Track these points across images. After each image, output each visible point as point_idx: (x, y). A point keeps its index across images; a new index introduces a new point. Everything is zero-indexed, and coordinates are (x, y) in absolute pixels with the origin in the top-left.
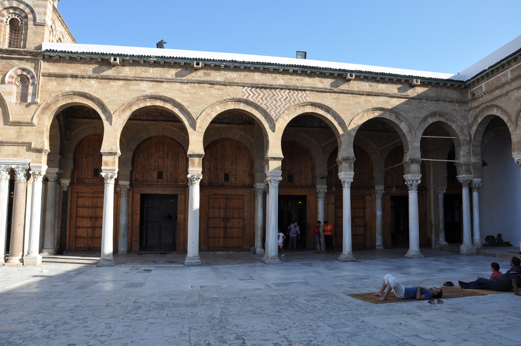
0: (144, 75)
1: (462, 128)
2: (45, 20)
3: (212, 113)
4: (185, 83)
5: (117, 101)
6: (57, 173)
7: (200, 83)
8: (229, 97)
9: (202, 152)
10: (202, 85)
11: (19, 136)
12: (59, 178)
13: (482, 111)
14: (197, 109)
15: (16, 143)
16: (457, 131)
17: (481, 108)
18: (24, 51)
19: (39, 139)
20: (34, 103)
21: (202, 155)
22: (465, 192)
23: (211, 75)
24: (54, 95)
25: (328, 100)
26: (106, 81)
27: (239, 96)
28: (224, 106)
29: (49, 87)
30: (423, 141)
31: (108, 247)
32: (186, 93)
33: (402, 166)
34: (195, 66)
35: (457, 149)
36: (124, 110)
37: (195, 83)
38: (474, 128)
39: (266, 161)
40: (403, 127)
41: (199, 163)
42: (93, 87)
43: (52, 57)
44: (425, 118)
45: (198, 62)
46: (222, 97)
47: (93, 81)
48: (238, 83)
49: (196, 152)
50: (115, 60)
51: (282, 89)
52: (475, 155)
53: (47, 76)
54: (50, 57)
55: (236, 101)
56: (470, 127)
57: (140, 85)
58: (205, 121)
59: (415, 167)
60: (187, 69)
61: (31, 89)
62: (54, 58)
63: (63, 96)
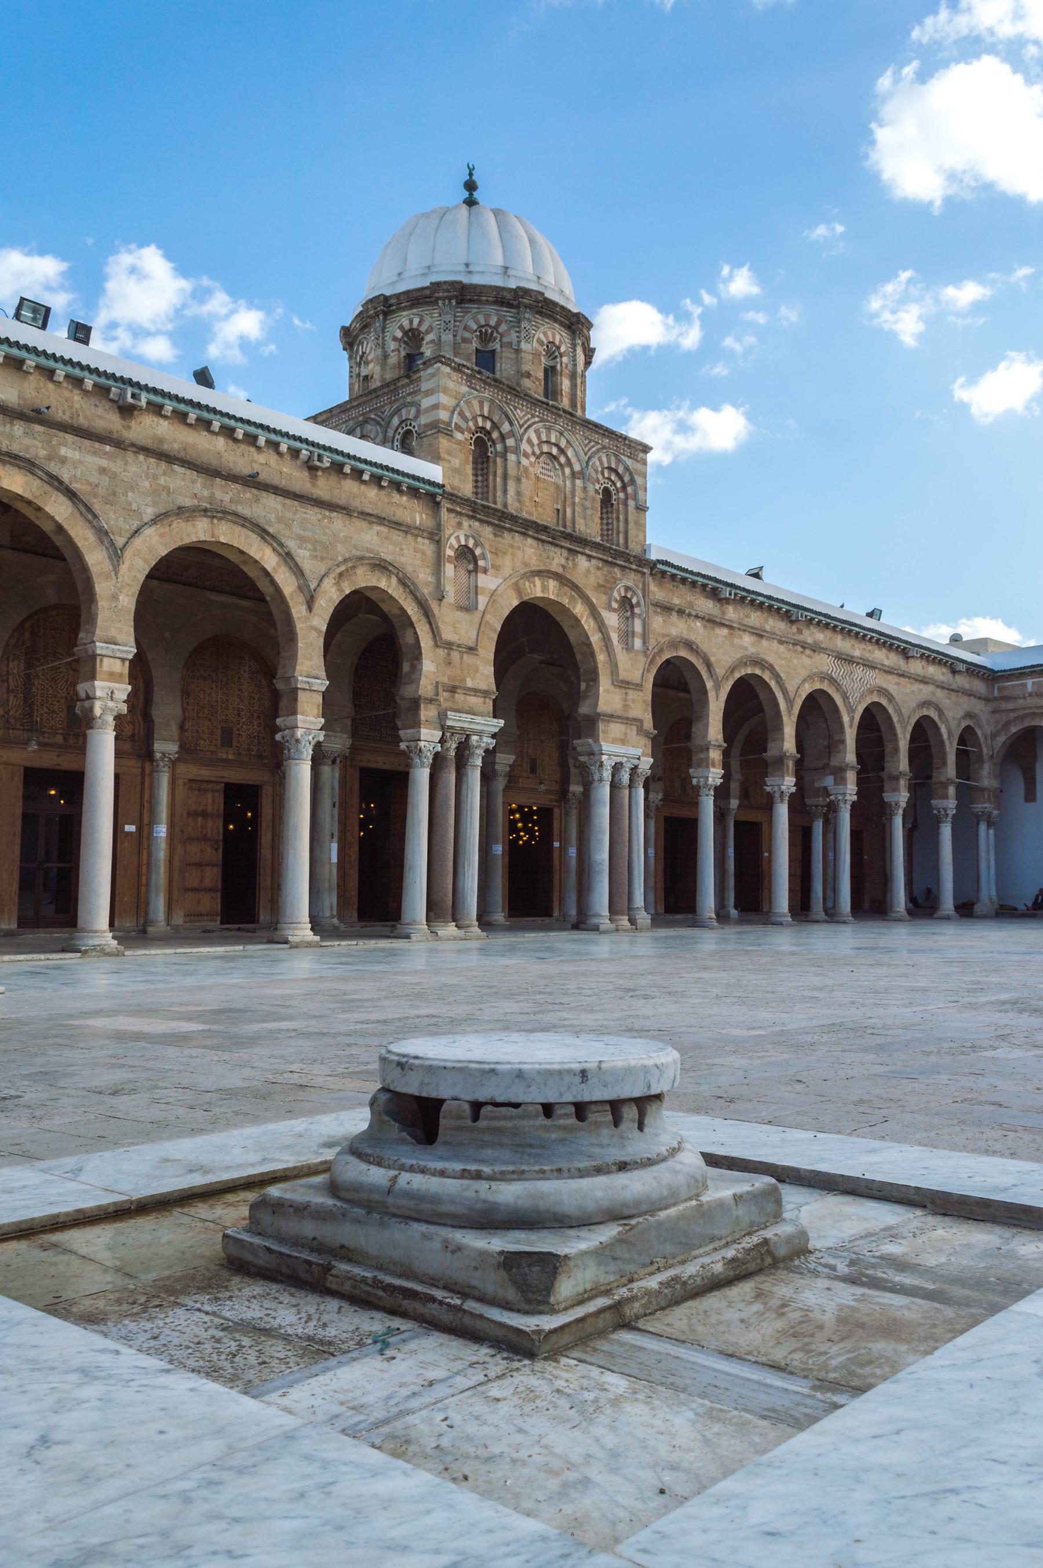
0: (747, 621)
1: (986, 738)
11: (626, 707)
16: (982, 740)
17: (1021, 713)
22: (983, 827)
25: (890, 683)
27: (825, 669)
38: (1002, 739)
39: (839, 773)
40: (943, 730)
47: (698, 624)
51: (858, 664)
54: (663, 573)
56: (994, 736)
59: (952, 790)
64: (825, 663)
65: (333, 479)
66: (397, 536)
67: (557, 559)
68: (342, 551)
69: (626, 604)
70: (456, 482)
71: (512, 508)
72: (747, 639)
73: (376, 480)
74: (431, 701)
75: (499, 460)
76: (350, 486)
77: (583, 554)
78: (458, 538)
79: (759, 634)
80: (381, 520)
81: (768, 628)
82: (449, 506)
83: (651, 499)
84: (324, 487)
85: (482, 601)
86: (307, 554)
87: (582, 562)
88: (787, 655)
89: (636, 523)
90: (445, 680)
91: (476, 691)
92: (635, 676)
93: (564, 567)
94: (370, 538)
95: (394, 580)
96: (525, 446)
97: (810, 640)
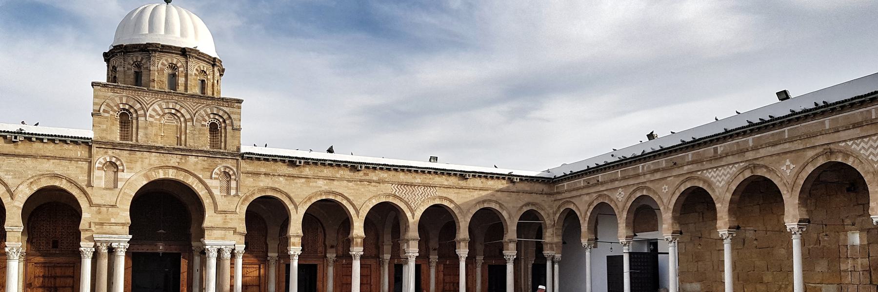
13: (564, 203)
25: (452, 194)
27: (389, 192)
30: (519, 226)
33: (502, 244)
35: (544, 231)
38: (558, 215)
39: (407, 241)
40: (505, 214)
43: (250, 157)
44: (521, 207)
47: (281, 179)
52: (557, 236)
56: (555, 214)
59: (513, 246)
61: (233, 184)
64: (389, 188)
65: (28, 143)
66: (64, 162)
67: (174, 160)
68: (30, 173)
69: (226, 173)
70: (104, 135)
71: (141, 142)
72: (321, 183)
75: (134, 121)
76: (38, 145)
79: (332, 179)
80: (55, 158)
81: (338, 176)
83: (243, 125)
84: (22, 148)
85: (120, 185)
87: (192, 159)
88: (356, 187)
89: (232, 136)
92: (232, 208)
94: (49, 166)
95: (64, 181)
96: (150, 112)
97: (375, 178)
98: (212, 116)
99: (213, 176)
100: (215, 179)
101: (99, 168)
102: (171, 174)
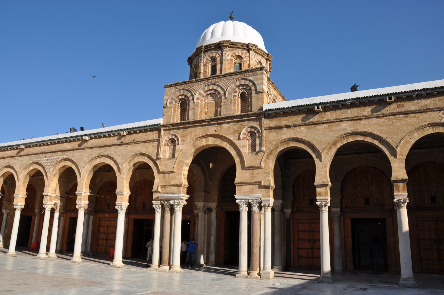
0: (343, 116)
2: (263, 88)
3: (411, 140)
4: (381, 117)
5: (325, 141)
6: (281, 205)
7: (394, 114)
8: (426, 123)
9: (406, 177)
10: (397, 116)
12: (283, 208)
14: (395, 139)
15: (251, 183)
18: (251, 114)
19: (267, 178)
20: (261, 151)
21: (406, 180)
23: (405, 105)
24: (275, 143)
26: (313, 126)
27: (437, 120)
28: (422, 132)
29: (270, 137)
31: (327, 266)
32: (383, 126)
34: (388, 100)
36: (330, 148)
37: (390, 116)
41: (404, 187)
42: (303, 133)
45: (390, 96)
46: (418, 124)
47: (302, 128)
48: (433, 108)
49: (400, 178)
50: (318, 108)
53: (268, 129)
54: (269, 114)
55: (434, 126)
57: (342, 125)
58: (404, 148)
60: (380, 105)
62: (272, 115)
63: (281, 143)
65: (130, 136)
66: (147, 144)
67: (212, 129)
68: (130, 154)
73: (141, 132)
74: (156, 192)
77: (225, 123)
78: (169, 137)
82: (164, 128)
85: (177, 154)
86: (120, 158)
87: (226, 126)
89: (257, 99)
90: (163, 184)
91: (174, 186)
93: (215, 130)
95: (146, 158)
97: (413, 108)
98: (241, 87)
99: (241, 136)
100: (243, 138)
101: (165, 145)
102: (211, 141)
